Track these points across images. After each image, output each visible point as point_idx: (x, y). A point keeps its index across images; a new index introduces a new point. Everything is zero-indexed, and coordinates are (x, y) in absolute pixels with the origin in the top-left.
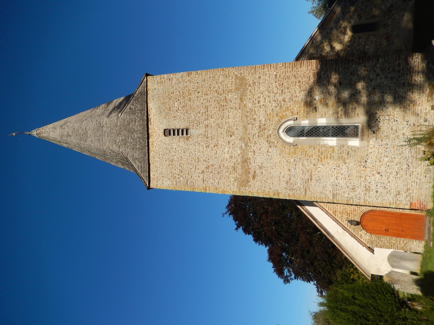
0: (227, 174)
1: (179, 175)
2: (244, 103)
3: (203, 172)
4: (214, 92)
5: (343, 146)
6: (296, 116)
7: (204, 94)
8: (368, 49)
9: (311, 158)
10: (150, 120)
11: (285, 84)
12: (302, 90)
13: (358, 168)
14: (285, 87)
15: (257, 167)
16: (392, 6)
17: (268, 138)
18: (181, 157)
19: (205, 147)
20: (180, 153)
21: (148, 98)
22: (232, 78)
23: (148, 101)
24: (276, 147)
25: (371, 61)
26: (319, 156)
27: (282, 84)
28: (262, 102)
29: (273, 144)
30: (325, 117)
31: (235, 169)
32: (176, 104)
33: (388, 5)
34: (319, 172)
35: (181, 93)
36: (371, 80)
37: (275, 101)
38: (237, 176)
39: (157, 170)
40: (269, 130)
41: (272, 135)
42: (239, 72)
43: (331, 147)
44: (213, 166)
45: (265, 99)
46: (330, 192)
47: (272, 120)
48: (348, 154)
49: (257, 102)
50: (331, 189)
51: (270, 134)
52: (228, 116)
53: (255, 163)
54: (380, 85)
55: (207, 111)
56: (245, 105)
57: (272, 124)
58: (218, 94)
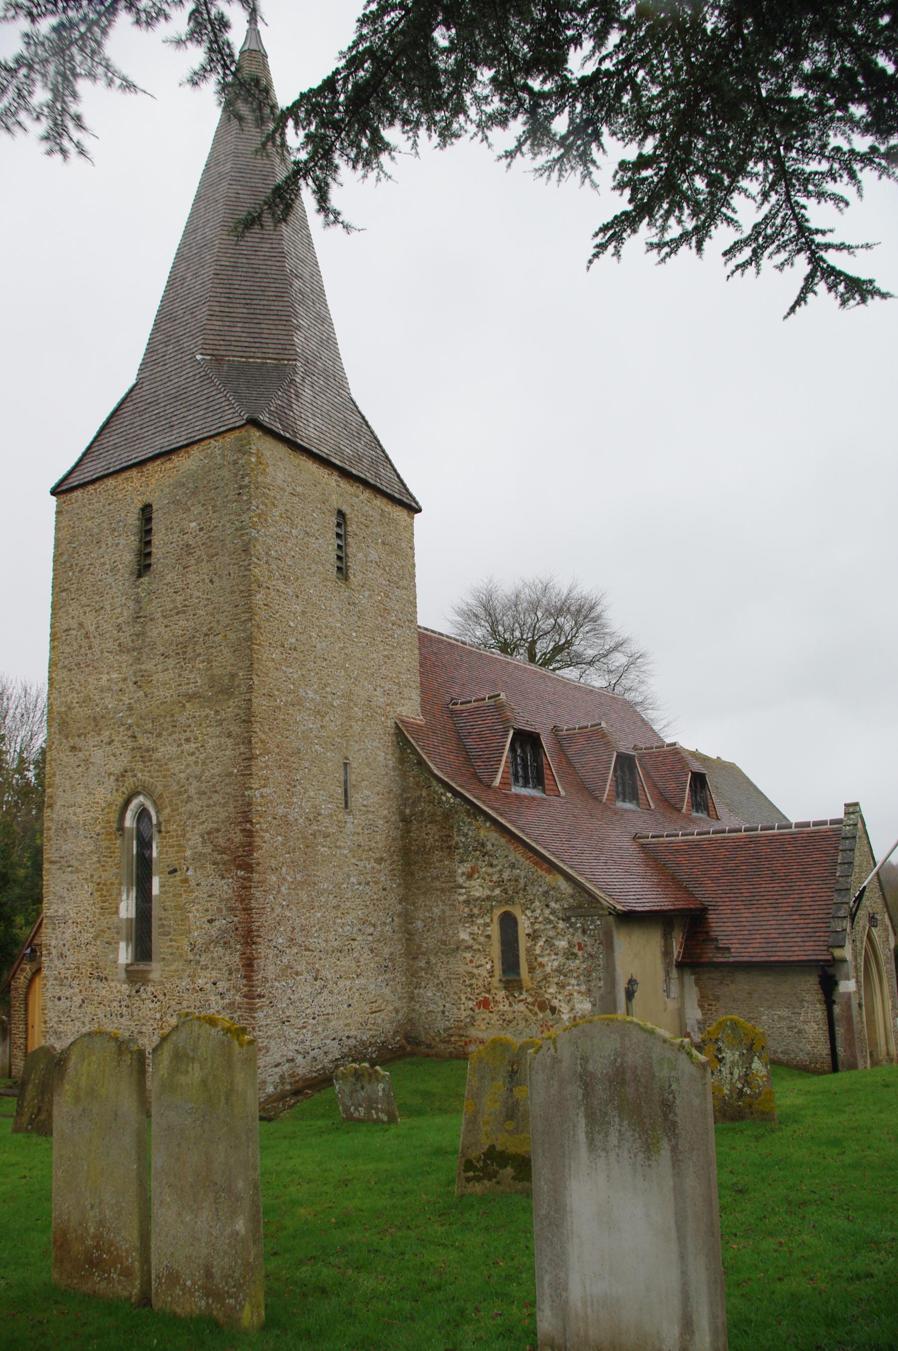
0: (77, 686)
1: (77, 565)
2: (188, 705)
3: (81, 625)
4: (210, 623)
5: (118, 933)
6: (163, 829)
7: (209, 597)
8: (465, 958)
9: (101, 869)
10: (170, 459)
11: (216, 797)
12: (203, 838)
13: (89, 963)
14: (210, 798)
15: (87, 753)
16: (553, 1010)
17: (132, 770)
18: (104, 564)
19: (120, 620)
20: (110, 559)
21: (207, 442)
22: (232, 665)
23: (202, 444)
24: (117, 790)
25: (245, 982)
26: (105, 885)
27: (216, 792)
28: (187, 747)
29: (121, 784)
30: (161, 892)
31: (84, 702)
32: (194, 524)
33: (555, 1003)
34: (82, 886)
35: (213, 534)
36: (215, 984)
37: (188, 779)
38: (74, 708)
39: (84, 506)
40: (142, 771)
41: (135, 779)
42: (242, 682)
43: (117, 908)
44: (90, 648)
45: (193, 754)
46: (57, 911)
47: (158, 777)
48: (107, 943)
49: (188, 734)
50: (61, 911)
51: (135, 776)
52: (167, 670)
53: (94, 746)
54: (208, 1001)
55: (177, 614)
56: (184, 706)
57: (152, 777)
58: (206, 635)
